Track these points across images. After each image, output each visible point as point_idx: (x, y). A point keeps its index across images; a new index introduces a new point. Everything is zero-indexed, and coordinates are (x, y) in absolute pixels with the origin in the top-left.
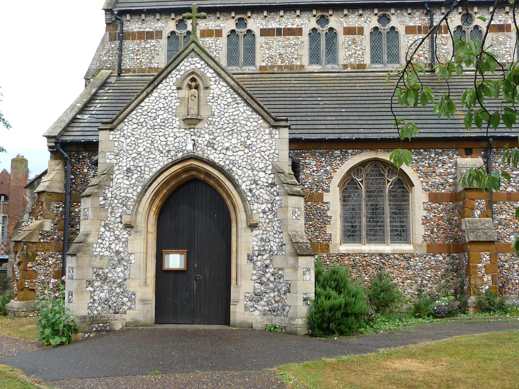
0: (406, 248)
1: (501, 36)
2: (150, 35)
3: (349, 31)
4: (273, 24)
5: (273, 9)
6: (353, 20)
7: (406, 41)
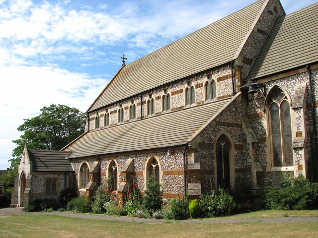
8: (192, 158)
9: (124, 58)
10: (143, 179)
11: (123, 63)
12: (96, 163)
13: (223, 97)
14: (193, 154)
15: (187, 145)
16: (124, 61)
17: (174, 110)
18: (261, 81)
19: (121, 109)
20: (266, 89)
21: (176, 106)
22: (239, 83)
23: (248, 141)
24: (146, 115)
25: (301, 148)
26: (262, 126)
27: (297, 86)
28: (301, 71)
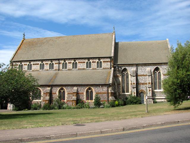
0: (40, 101)
1: (70, 64)
2: (16, 65)
3: (46, 64)
4: (35, 63)
5: (34, 61)
6: (47, 62)
7: (55, 65)
8: (110, 90)
9: (24, 35)
10: (84, 95)
11: (23, 37)
12: (50, 88)
13: (105, 68)
14: (111, 87)
15: (109, 84)
16: (24, 36)
17: (79, 69)
18: (120, 66)
19: (42, 64)
20: (121, 68)
21: (80, 68)
22: (113, 65)
23: (116, 84)
24: (62, 68)
25: (135, 88)
26: (119, 80)
27: (133, 69)
28: (134, 65)
